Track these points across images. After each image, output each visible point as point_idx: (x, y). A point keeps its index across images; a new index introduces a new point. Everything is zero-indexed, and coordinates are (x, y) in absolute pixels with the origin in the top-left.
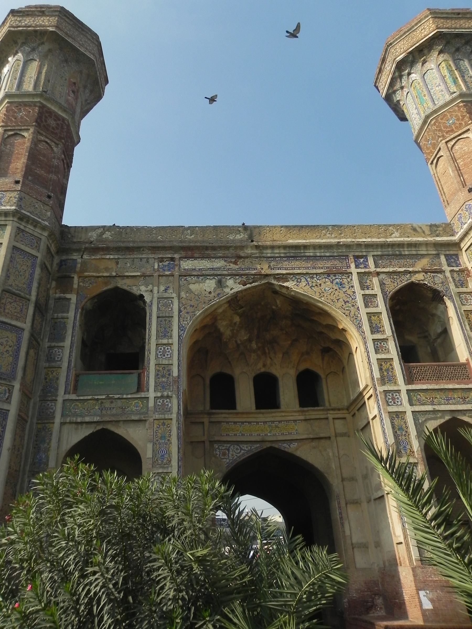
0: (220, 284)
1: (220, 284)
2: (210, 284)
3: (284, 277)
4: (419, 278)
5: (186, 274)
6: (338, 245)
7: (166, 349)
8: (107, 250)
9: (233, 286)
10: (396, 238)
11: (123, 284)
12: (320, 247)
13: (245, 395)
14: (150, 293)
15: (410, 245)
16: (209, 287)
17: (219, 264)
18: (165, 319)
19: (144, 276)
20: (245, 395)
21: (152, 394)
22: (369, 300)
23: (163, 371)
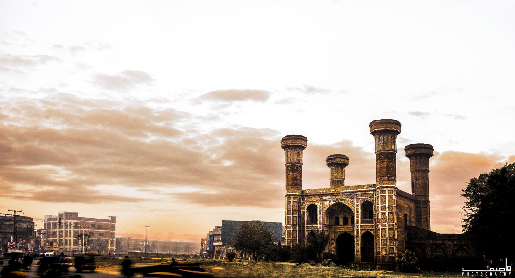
0: (330, 202)
1: (330, 202)
2: (328, 202)
3: (342, 200)
4: (368, 199)
5: (324, 200)
6: (352, 192)
7: (321, 217)
8: (310, 195)
9: (332, 203)
10: (365, 189)
11: (312, 203)
12: (349, 192)
13: (341, 222)
14: (318, 204)
15: (367, 191)
16: (328, 203)
17: (329, 197)
18: (320, 210)
19: (317, 201)
20: (341, 222)
21: (318, 225)
22: (357, 206)
23: (320, 221)
